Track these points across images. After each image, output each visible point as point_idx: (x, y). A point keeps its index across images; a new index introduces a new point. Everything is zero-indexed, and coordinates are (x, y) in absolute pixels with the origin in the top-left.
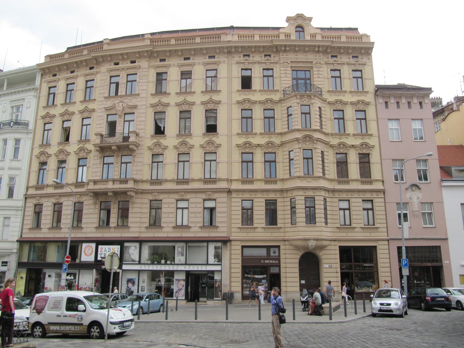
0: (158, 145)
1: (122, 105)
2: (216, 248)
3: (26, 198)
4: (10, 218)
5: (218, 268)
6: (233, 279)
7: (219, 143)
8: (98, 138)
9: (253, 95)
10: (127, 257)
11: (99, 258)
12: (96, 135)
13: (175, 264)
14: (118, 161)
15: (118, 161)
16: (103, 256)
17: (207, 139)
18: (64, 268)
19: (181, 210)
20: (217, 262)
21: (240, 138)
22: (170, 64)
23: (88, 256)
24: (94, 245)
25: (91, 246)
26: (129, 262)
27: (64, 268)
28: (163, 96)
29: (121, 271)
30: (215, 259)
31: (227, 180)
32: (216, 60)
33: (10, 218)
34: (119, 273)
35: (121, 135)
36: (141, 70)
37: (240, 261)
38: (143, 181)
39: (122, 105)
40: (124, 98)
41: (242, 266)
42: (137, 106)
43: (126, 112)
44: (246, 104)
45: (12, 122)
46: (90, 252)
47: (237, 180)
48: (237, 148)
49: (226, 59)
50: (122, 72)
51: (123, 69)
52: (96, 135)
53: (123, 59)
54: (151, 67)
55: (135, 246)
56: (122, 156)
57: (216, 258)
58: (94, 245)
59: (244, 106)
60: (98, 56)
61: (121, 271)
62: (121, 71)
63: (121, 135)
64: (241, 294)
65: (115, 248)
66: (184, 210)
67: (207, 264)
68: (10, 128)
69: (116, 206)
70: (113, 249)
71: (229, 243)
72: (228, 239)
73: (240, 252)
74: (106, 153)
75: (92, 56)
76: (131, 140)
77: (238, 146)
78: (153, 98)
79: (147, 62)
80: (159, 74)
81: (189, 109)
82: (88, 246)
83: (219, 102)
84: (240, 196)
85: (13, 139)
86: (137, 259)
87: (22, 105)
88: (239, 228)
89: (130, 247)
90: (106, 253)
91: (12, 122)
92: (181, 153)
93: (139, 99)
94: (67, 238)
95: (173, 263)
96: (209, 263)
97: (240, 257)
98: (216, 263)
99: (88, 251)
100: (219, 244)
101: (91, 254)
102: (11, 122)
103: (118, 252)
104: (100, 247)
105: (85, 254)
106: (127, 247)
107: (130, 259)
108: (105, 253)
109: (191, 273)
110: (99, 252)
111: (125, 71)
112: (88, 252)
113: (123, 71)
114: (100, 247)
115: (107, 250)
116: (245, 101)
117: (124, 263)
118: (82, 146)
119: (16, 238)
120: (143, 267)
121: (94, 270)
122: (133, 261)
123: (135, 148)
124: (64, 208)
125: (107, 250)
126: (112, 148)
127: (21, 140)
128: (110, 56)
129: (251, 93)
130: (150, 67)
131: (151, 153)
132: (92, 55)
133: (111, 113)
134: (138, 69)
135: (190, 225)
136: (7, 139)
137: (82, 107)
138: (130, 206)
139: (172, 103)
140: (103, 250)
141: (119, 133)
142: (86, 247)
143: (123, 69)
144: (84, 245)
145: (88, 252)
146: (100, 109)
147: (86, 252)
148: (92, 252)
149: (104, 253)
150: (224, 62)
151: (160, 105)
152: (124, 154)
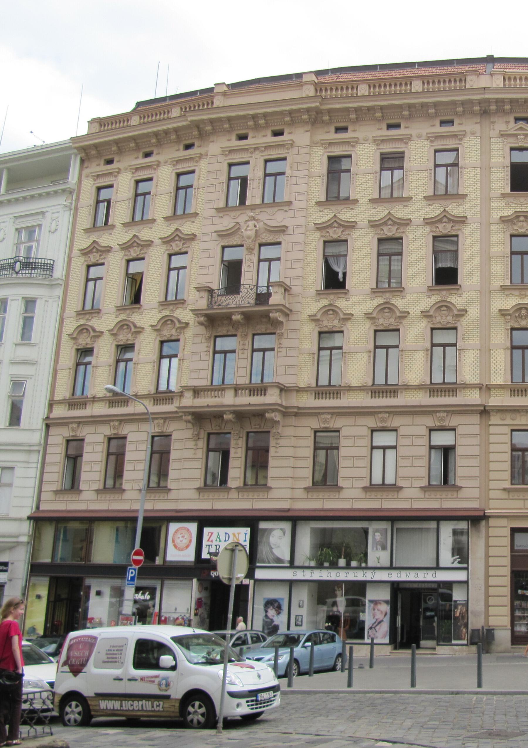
0: (331, 312)
1: (255, 226)
2: (455, 533)
3: (48, 426)
4: (12, 468)
5: (461, 576)
6: (492, 601)
7: (463, 308)
8: (202, 297)
10: (264, 553)
11: (205, 555)
12: (198, 291)
13: (367, 568)
14: (246, 347)
15: (246, 347)
16: (213, 550)
17: (436, 298)
18: (130, 575)
19: (381, 451)
20: (459, 562)
21: (507, 296)
22: (357, 138)
23: (181, 550)
24: (193, 527)
25: (188, 530)
26: (269, 563)
27: (130, 575)
28: (343, 206)
29: (252, 582)
30: (453, 556)
31: (480, 387)
32: (456, 128)
33: (12, 468)
34: (247, 586)
35: (252, 289)
36: (295, 150)
37: (507, 561)
38: (299, 390)
39: (255, 226)
40: (258, 211)
41: (513, 572)
42: (287, 227)
43: (264, 241)
44: (520, 224)
45: (18, 264)
46: (185, 542)
48: (502, 319)
49: (477, 127)
50: (253, 155)
51: (256, 149)
52: (199, 289)
53: (257, 127)
54: (318, 143)
55: (281, 529)
56: (254, 335)
57: (456, 553)
58: (193, 527)
59: (515, 228)
60: (203, 121)
61: (252, 582)
62: (252, 153)
63: (252, 289)
64: (510, 631)
65: (239, 534)
66: (387, 451)
67: (438, 567)
68: (15, 276)
69: (242, 442)
70: (234, 534)
71: (483, 523)
72: (482, 514)
73: (507, 541)
74: (220, 329)
75: (190, 121)
76: (273, 300)
77: (503, 313)
78: (321, 211)
79: (308, 134)
80: (333, 160)
81: (398, 235)
82: (181, 528)
83: (462, 220)
84: (508, 421)
85: (20, 299)
86: (287, 557)
87: (40, 226)
88: (504, 489)
89: (271, 530)
90: (220, 544)
91: (18, 264)
92: (382, 328)
93: (291, 213)
94: (137, 511)
95: (363, 565)
96: (442, 565)
97: (507, 551)
98: (456, 565)
99: (181, 539)
100: (463, 525)
101: (187, 547)
102: (16, 262)
103: (245, 541)
104: (207, 530)
105: (176, 547)
106: (265, 530)
107: (271, 557)
108: (217, 543)
109: (401, 586)
110: (205, 542)
111: (262, 151)
112: (182, 541)
113: (257, 152)
114: (207, 530)
115: (223, 538)
116: (518, 217)
117: (258, 564)
118: (168, 313)
119: (27, 512)
120: (299, 575)
121: (195, 580)
122: (279, 560)
123: (281, 319)
124: (129, 447)
125: (223, 538)
126: (234, 317)
127: (38, 301)
128: (229, 119)
130: (313, 144)
131: (317, 329)
132: (190, 119)
133: (231, 244)
134: (288, 149)
135: (400, 483)
136: (7, 299)
137: (167, 230)
138: (272, 442)
139: (363, 222)
140: (214, 537)
141: (248, 286)
142: (178, 530)
143: (256, 149)
144: (173, 527)
145: (182, 541)
146: (207, 234)
147: (178, 541)
148: (190, 541)
149: (215, 543)
150: (473, 133)
151: (335, 225)
152: (259, 332)
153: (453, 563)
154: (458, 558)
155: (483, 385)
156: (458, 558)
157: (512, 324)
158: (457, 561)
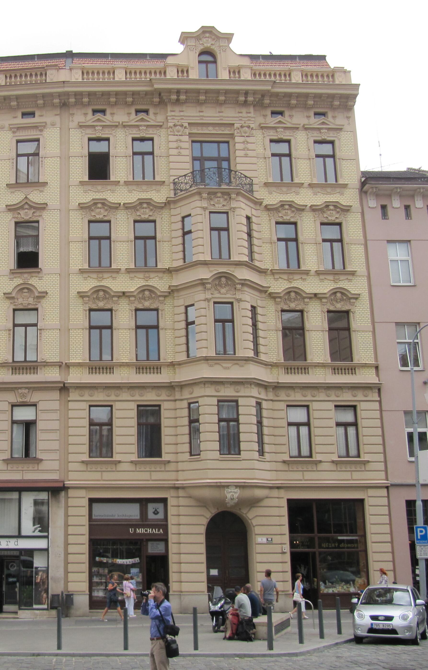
6: (71, 567)
7: (43, 290)
9: (113, 191)
17: (18, 281)
20: (40, 531)
21: (85, 279)
30: (34, 525)
31: (60, 365)
37: (85, 530)
47: (79, 365)
57: (36, 523)
59: (93, 214)
64: (87, 597)
67: (19, 536)
71: (63, 494)
72: (61, 485)
73: (85, 511)
84: (86, 398)
88: (83, 462)
96: (23, 533)
97: (85, 521)
98: (37, 533)
116: (95, 204)
129: (109, 187)
153: (34, 532)
154: (39, 527)
155: (62, 363)
156: (39, 527)
157: (90, 306)
158: (38, 530)
